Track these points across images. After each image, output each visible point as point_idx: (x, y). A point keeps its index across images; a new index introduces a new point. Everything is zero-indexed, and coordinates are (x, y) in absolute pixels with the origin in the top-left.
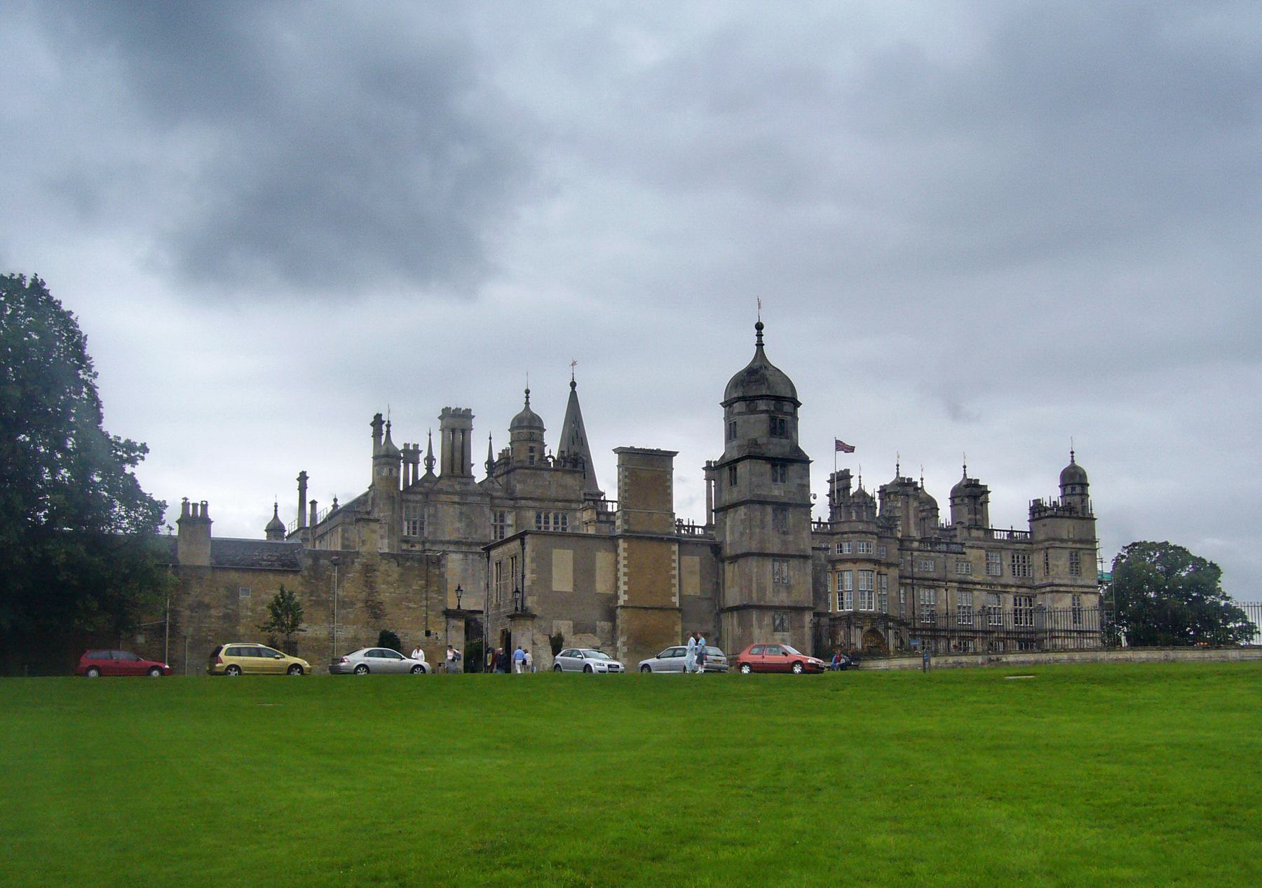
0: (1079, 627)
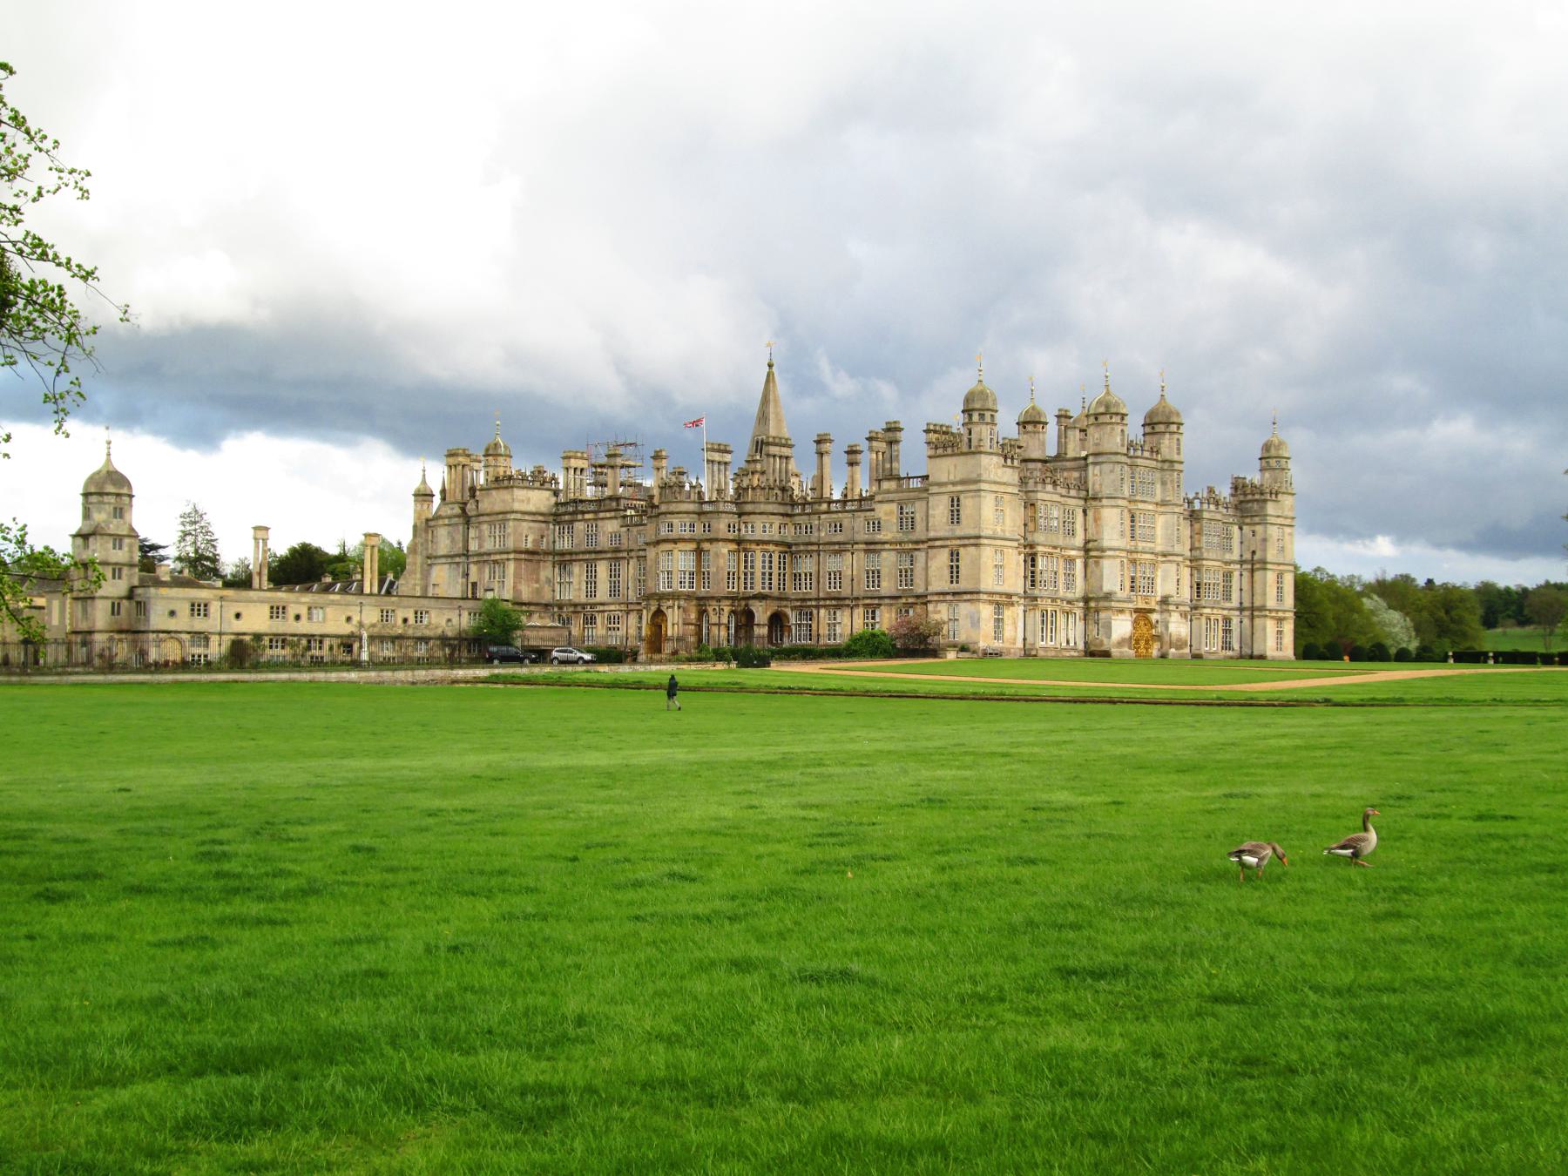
0: (955, 587)
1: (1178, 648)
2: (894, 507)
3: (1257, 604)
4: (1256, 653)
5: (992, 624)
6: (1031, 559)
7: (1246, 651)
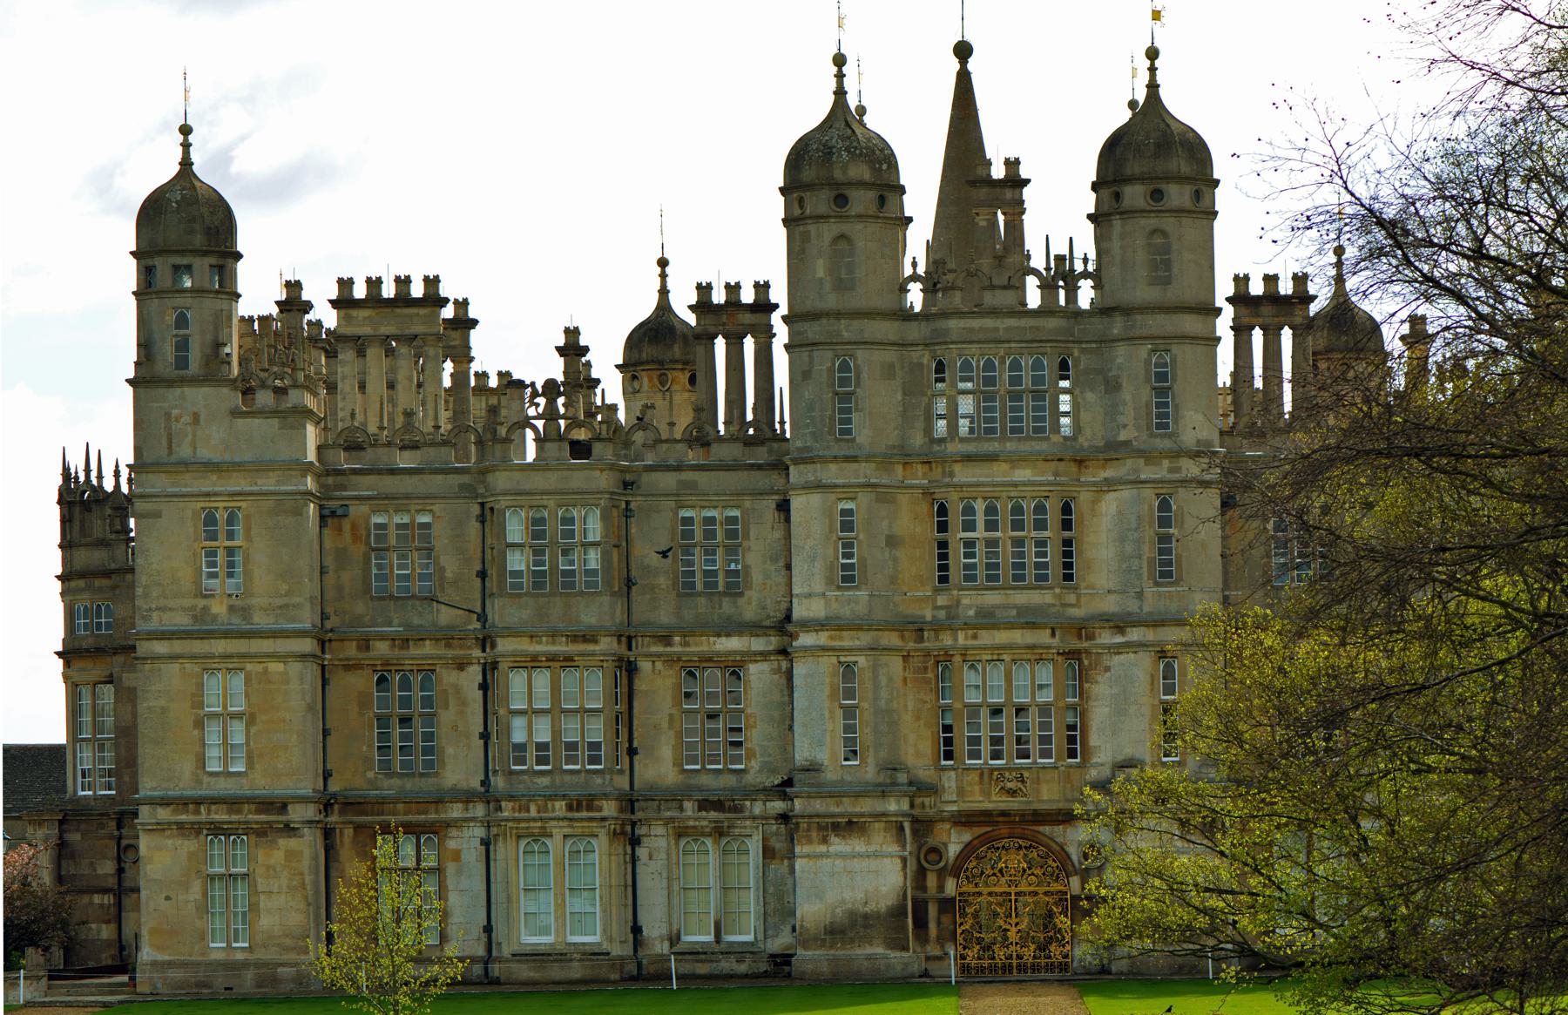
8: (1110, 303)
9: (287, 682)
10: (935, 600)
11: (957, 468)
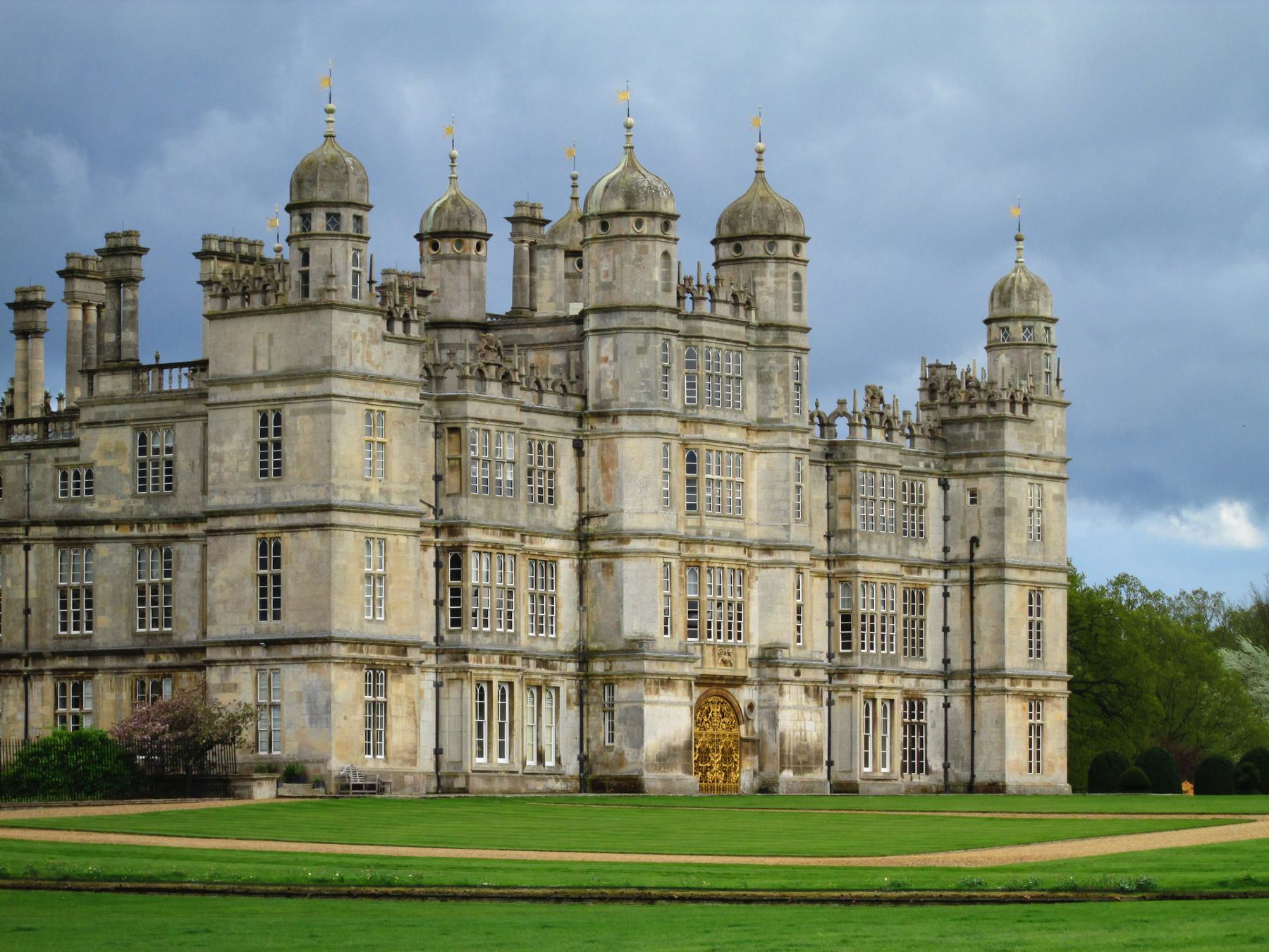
0: (271, 628)
1: (802, 767)
2: (125, 436)
3: (983, 663)
4: (982, 777)
5: (360, 714)
6: (452, 560)
7: (960, 773)
8: (763, 320)
9: (407, 551)
10: (686, 522)
11: (705, 427)
